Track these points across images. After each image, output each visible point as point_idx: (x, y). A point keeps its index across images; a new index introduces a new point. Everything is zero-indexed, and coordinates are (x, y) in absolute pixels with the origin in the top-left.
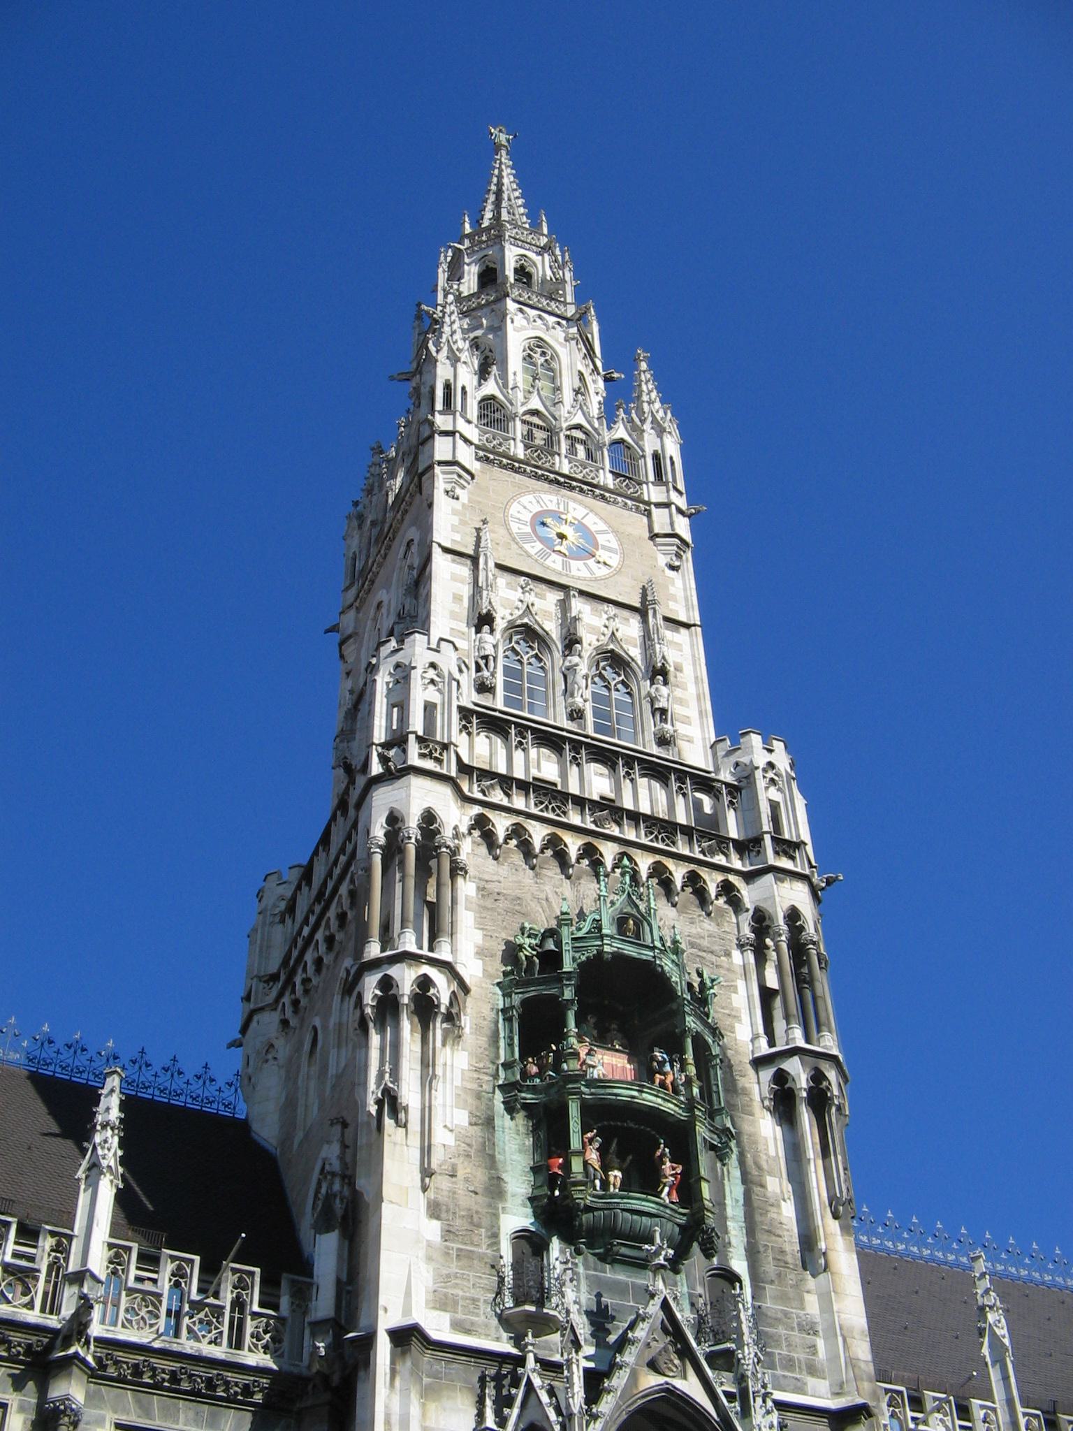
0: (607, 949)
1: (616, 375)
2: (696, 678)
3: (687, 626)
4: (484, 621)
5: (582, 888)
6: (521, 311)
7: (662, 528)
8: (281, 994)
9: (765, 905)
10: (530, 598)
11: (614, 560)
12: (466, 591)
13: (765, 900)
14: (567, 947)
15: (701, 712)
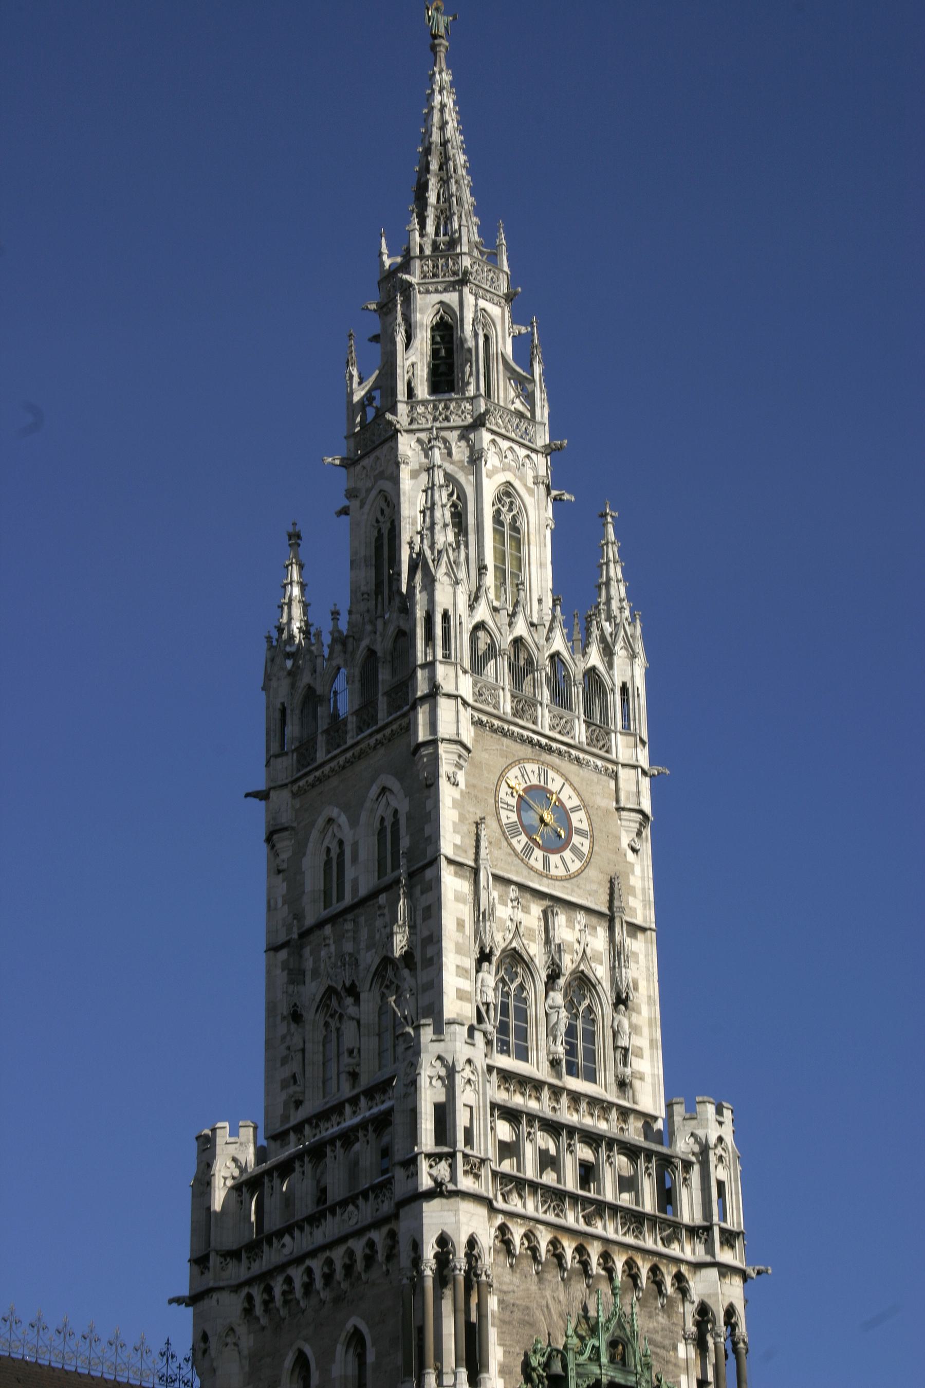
0: (605, 1380)
1: (566, 497)
2: (649, 997)
3: (643, 930)
4: (484, 957)
5: (572, 1290)
6: (493, 441)
7: (628, 798)
8: (249, 1282)
9: (710, 1302)
10: (519, 915)
11: (585, 849)
12: (466, 912)
13: (709, 1296)
14: (572, 1374)
15: (651, 1041)
